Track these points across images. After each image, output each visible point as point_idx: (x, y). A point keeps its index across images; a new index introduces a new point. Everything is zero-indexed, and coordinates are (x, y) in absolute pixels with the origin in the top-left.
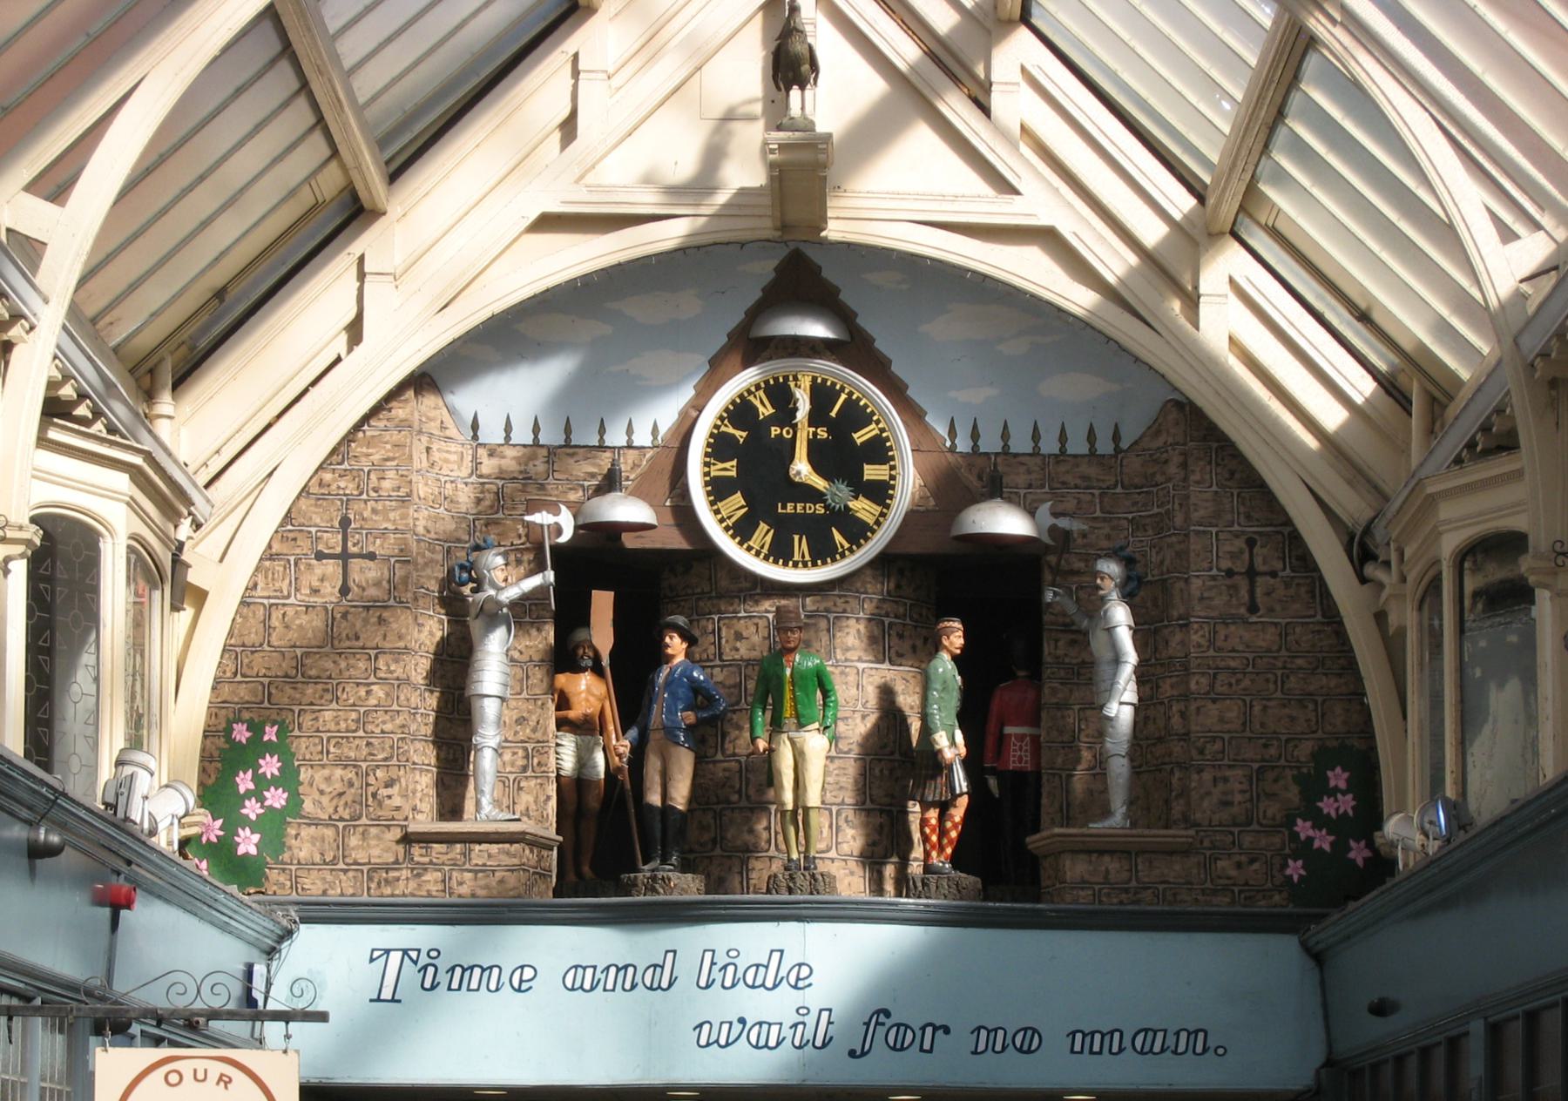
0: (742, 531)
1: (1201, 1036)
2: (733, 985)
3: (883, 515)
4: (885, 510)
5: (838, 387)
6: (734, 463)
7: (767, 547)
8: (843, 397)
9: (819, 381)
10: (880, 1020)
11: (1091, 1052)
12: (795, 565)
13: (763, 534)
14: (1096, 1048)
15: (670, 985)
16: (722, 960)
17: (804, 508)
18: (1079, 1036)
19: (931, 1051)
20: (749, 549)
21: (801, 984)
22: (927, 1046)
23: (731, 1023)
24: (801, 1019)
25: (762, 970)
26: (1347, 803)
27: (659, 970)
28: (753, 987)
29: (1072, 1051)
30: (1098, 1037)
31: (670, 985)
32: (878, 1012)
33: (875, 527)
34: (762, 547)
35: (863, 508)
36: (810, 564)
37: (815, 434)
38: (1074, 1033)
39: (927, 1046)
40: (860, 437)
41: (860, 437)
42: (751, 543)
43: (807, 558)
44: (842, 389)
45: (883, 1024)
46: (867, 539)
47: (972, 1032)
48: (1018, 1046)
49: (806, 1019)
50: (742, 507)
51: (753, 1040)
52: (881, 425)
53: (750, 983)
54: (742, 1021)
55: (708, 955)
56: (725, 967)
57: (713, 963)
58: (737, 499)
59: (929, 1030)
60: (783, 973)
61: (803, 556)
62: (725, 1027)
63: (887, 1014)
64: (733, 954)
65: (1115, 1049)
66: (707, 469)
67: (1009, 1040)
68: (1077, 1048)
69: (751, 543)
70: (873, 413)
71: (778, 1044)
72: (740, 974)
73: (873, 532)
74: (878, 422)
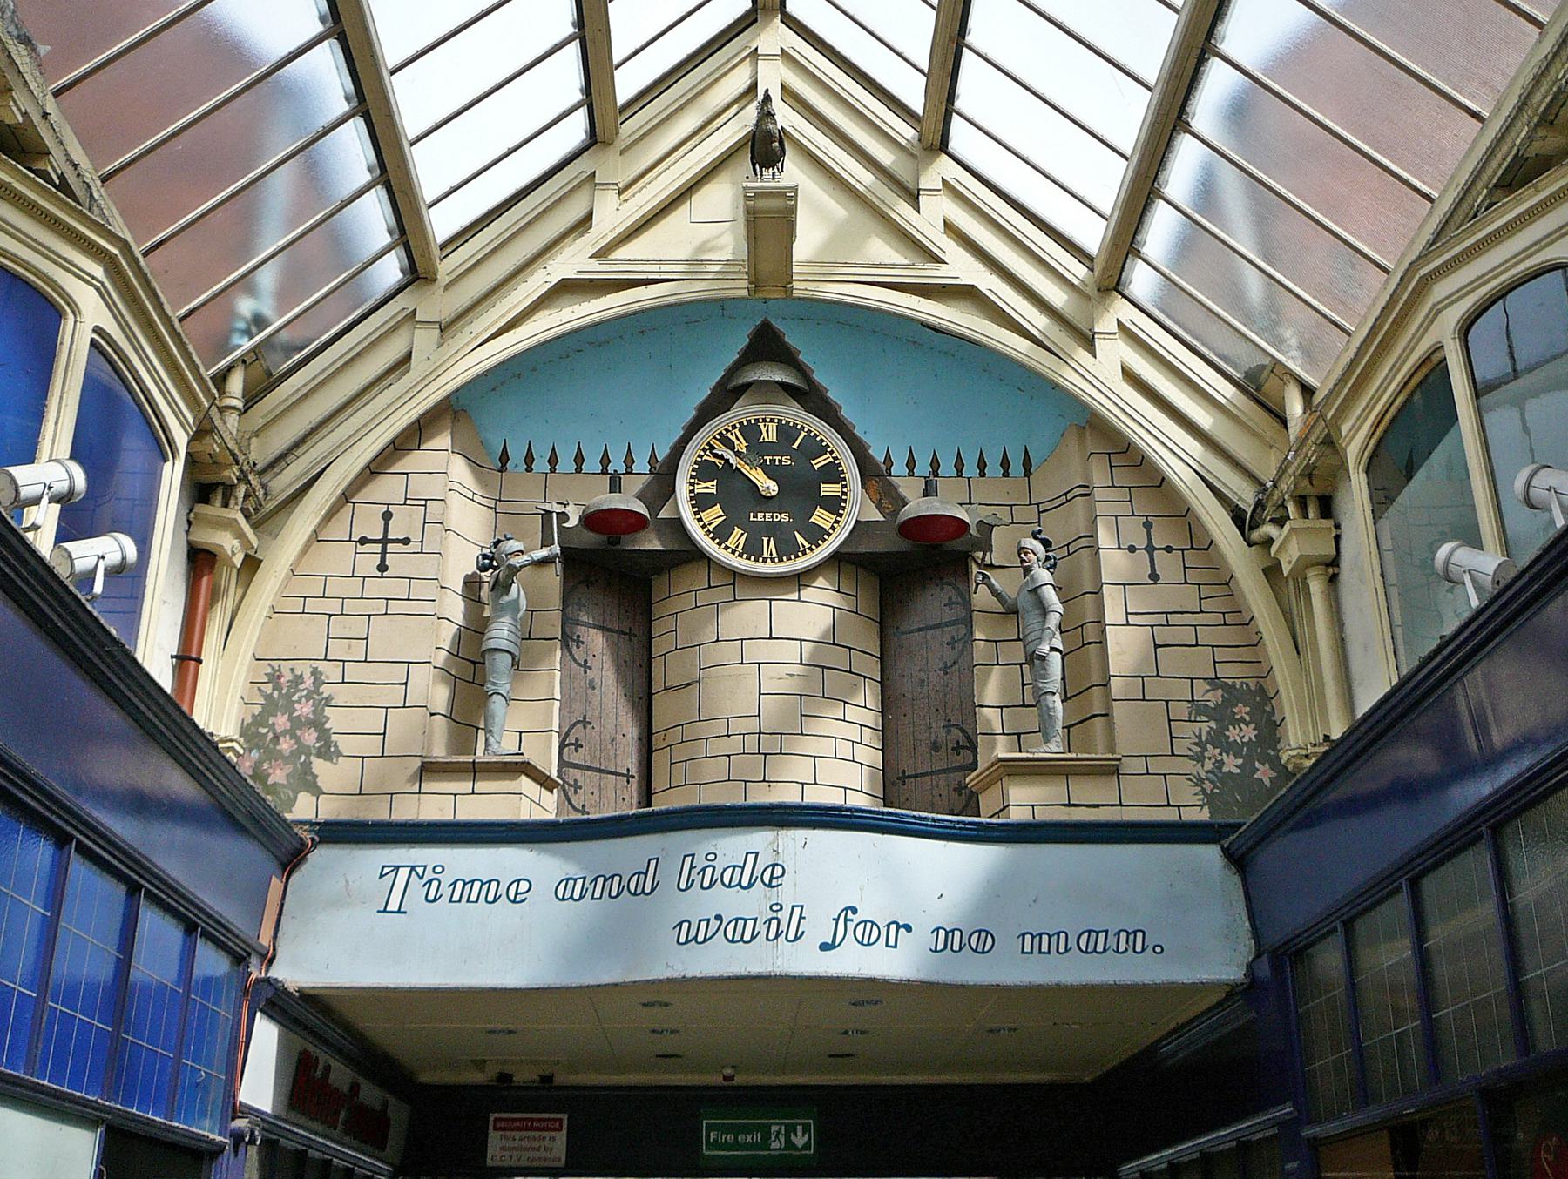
0: (720, 534)
1: (1139, 935)
2: (711, 886)
3: (837, 522)
4: (839, 519)
5: (799, 427)
6: (715, 483)
7: (741, 546)
8: (803, 434)
9: (784, 422)
10: (848, 917)
11: (1040, 952)
12: (765, 560)
13: (737, 537)
14: (1045, 948)
15: (653, 889)
16: (700, 863)
17: (772, 517)
18: (1028, 937)
19: (895, 946)
20: (726, 548)
21: (774, 883)
22: (891, 942)
23: (708, 920)
24: (775, 915)
25: (738, 870)
26: (1250, 733)
27: (642, 877)
28: (729, 886)
29: (1023, 952)
30: (1045, 938)
31: (653, 889)
32: (846, 909)
33: (831, 531)
34: (737, 547)
35: (821, 518)
36: (776, 560)
37: (780, 461)
38: (1023, 935)
39: (891, 942)
40: (817, 463)
41: (817, 463)
42: (728, 544)
43: (775, 555)
44: (803, 428)
45: (852, 920)
46: (824, 540)
47: (932, 932)
48: (974, 947)
49: (779, 915)
50: (721, 516)
51: (730, 937)
52: (834, 455)
53: (726, 882)
54: (719, 917)
55: (688, 859)
56: (704, 870)
57: (692, 868)
58: (717, 510)
59: (893, 927)
60: (757, 873)
61: (771, 554)
62: (704, 924)
63: (855, 911)
64: (711, 857)
65: (1062, 949)
66: (692, 488)
67: (965, 940)
68: (1027, 949)
69: (728, 544)
70: (828, 446)
71: (753, 938)
72: (717, 875)
73: (829, 535)
74: (832, 452)
